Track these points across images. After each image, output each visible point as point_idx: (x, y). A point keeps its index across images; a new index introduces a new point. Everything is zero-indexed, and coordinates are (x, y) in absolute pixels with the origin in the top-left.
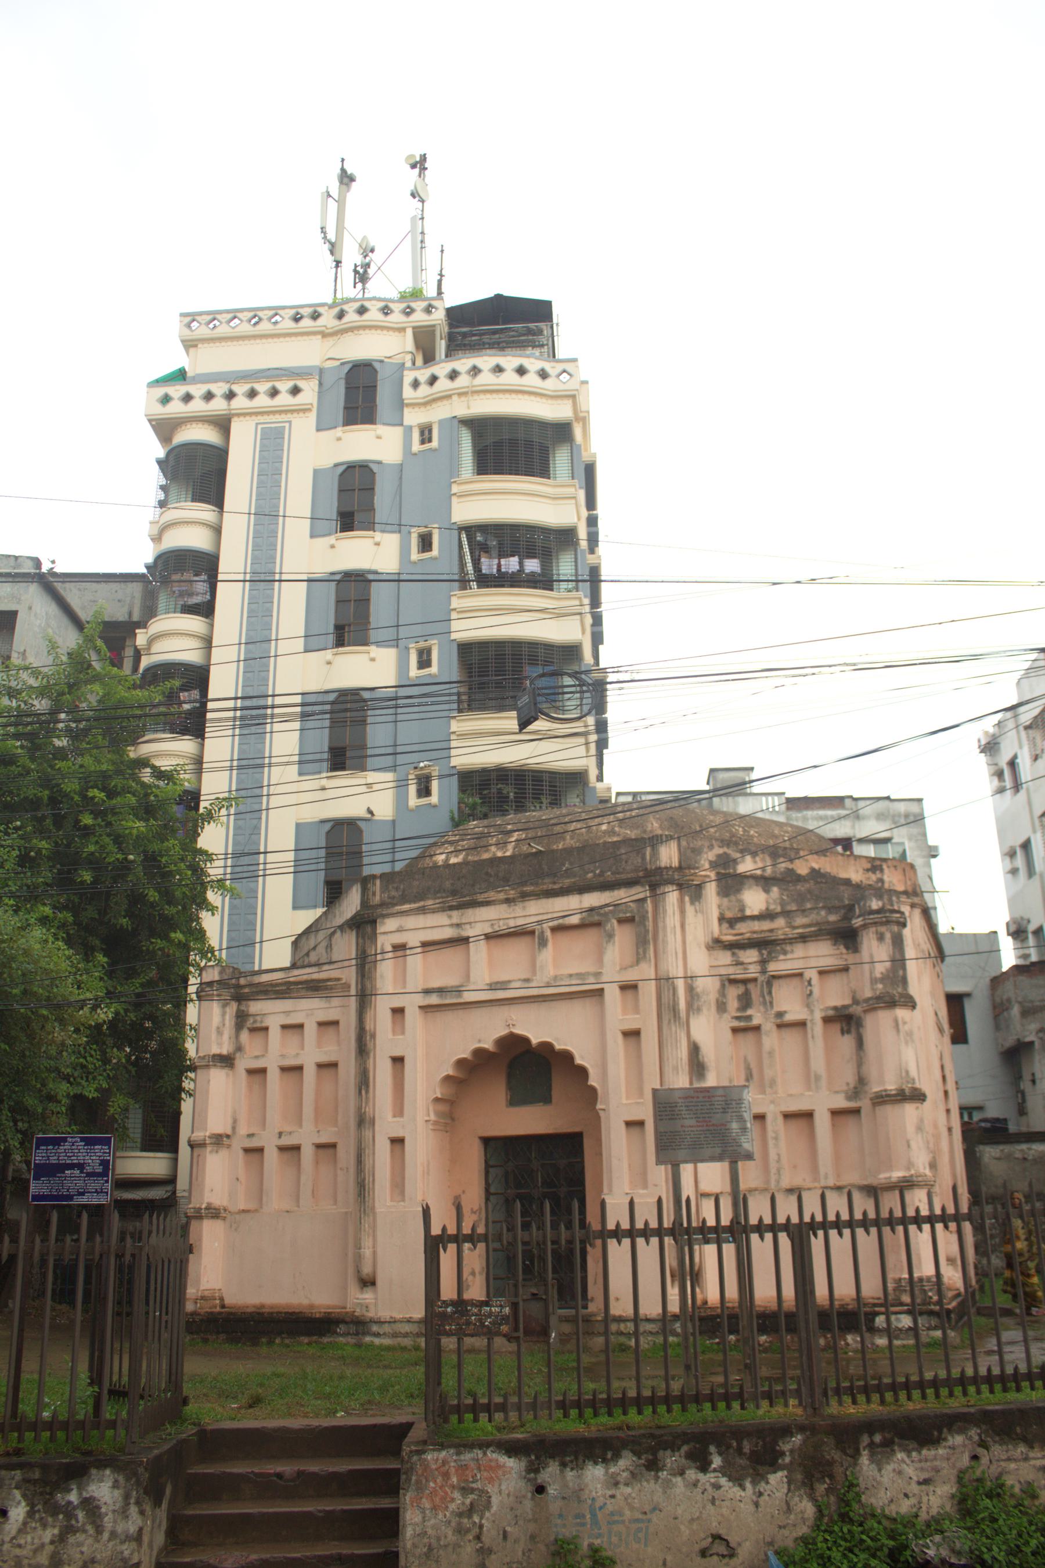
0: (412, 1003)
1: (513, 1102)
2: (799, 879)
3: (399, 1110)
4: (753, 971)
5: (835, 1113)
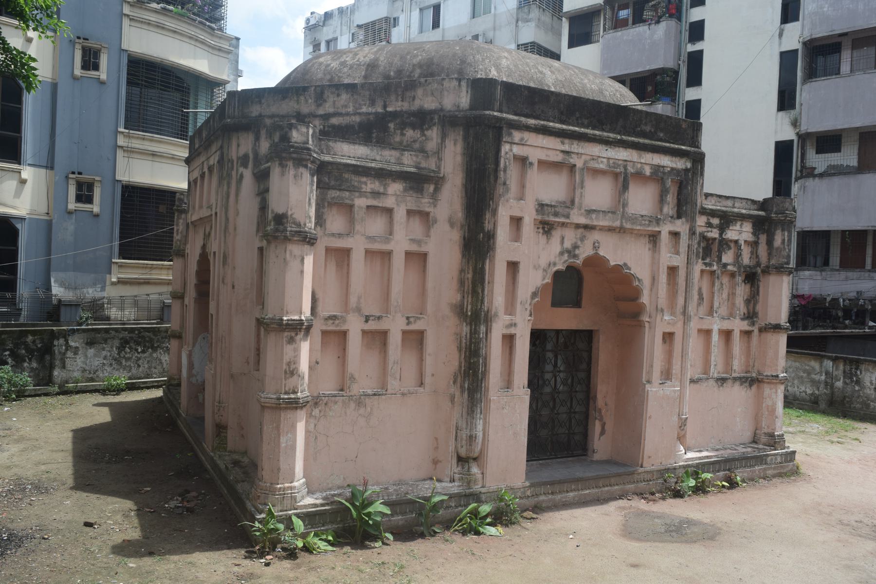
0: (529, 217)
3: (510, 309)
4: (714, 234)
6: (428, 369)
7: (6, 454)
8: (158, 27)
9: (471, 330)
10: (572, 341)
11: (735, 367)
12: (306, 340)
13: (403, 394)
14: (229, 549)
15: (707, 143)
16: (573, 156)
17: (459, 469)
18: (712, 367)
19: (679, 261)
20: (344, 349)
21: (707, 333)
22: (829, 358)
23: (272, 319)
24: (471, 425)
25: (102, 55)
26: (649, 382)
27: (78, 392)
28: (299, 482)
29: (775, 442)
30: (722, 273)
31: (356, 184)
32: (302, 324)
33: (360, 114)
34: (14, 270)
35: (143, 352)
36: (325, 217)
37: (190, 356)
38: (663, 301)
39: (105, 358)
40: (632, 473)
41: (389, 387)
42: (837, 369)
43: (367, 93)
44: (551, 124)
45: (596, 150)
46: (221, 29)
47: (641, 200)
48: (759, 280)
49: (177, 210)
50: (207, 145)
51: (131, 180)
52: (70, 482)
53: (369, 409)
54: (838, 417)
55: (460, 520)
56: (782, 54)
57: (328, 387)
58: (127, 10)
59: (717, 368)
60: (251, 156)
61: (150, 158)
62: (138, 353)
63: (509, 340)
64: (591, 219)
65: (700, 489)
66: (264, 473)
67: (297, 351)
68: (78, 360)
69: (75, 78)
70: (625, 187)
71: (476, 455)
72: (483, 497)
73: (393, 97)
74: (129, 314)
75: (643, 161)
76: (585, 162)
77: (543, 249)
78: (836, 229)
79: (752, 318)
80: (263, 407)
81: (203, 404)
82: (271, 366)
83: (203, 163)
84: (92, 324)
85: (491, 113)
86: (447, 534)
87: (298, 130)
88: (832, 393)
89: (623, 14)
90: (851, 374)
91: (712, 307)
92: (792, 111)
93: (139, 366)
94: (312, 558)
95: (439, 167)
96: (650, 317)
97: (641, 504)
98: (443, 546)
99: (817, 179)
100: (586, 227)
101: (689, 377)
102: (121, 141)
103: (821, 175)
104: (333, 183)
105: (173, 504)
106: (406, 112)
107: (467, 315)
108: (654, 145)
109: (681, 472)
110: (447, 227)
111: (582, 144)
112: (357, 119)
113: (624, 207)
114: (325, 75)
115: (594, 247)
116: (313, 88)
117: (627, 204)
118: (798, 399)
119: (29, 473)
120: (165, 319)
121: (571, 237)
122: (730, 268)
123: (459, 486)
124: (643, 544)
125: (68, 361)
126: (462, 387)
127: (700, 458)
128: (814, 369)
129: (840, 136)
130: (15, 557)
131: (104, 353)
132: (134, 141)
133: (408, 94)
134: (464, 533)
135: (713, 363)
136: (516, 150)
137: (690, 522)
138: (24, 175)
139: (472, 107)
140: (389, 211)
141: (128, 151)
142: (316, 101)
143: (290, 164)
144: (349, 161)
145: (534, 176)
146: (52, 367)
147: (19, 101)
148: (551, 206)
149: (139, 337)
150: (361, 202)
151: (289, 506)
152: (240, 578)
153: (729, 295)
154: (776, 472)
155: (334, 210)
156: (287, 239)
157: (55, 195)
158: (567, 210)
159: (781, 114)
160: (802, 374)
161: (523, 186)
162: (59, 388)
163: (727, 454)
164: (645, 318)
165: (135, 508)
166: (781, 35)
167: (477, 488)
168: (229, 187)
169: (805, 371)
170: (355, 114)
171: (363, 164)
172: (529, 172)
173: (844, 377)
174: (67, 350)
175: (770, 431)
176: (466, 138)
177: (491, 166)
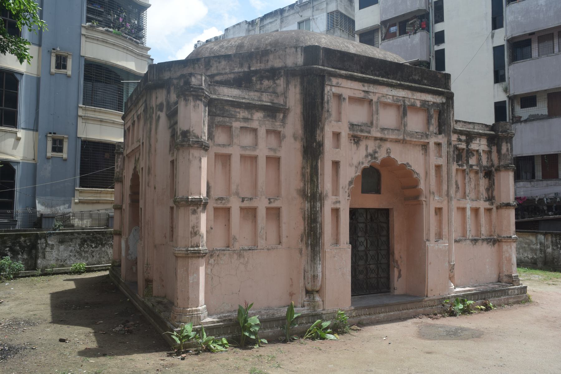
0: (345, 133)
1: (363, 192)
3: (336, 192)
4: (463, 146)
6: (284, 233)
7: (7, 307)
8: (103, 42)
9: (311, 206)
10: (376, 216)
11: (482, 232)
12: (204, 212)
13: (268, 249)
14: (156, 352)
15: (455, 87)
16: (370, 94)
17: (307, 298)
18: (468, 232)
19: (442, 161)
20: (229, 220)
21: (463, 210)
22: (541, 233)
23: (182, 198)
24: (314, 268)
25: (68, 59)
26: (428, 240)
27: (53, 274)
28: (202, 307)
29: (513, 281)
30: (470, 171)
31: (233, 113)
32: (201, 201)
33: (233, 73)
34: (11, 195)
35: (96, 247)
36: (214, 134)
37: (127, 242)
38: (433, 187)
39: (71, 251)
40: (421, 301)
41: (259, 245)
42: (547, 240)
43: (238, 60)
44: (356, 74)
45: (385, 90)
46: (142, 43)
47: (415, 122)
48: (493, 176)
49: (117, 153)
50: (136, 104)
51: (87, 137)
52: (50, 319)
53: (246, 259)
54: (551, 271)
55: (310, 331)
56: (495, 48)
57: (219, 244)
58: (84, 31)
59: (471, 234)
60: (165, 103)
61: (99, 123)
62: (93, 248)
63: (336, 212)
64: (384, 134)
65: (466, 311)
66: (179, 301)
67: (198, 219)
68: (54, 253)
69: (51, 74)
70: (405, 114)
71: (318, 289)
72: (324, 317)
73: (254, 61)
74: (86, 223)
75: (415, 98)
76: (378, 98)
77: (355, 153)
78: (538, 154)
79: (491, 200)
80: (177, 257)
81: (136, 273)
82: (181, 231)
83: (134, 115)
84: (62, 230)
85: (317, 66)
86: (302, 340)
87: (195, 77)
88: (546, 256)
89: (393, 29)
90: (557, 243)
91: (465, 193)
92: (504, 83)
93: (93, 256)
94: (213, 355)
95: (286, 103)
96: (426, 198)
97: (429, 321)
98: (299, 346)
99: (523, 123)
100: (381, 139)
101: (454, 239)
102: (81, 113)
103: (526, 121)
104: (218, 112)
105: (118, 329)
106: (263, 70)
107: (308, 196)
108: (422, 88)
109: (453, 300)
110: (292, 140)
111: (376, 86)
112: (232, 76)
113: (404, 127)
114: (210, 54)
115: (387, 152)
116: (203, 59)
117: (407, 125)
118: (523, 262)
119: (22, 316)
120: (110, 225)
121: (372, 146)
122: (474, 167)
123: (308, 310)
124: (433, 341)
125: (47, 253)
126: (307, 243)
127: (465, 291)
128: (532, 241)
129: (535, 96)
130: (13, 360)
131: (70, 248)
132: (89, 112)
133: (264, 59)
134: (313, 339)
135: (468, 230)
136: (334, 90)
137: (463, 329)
138: (19, 135)
139: (305, 63)
140: (255, 131)
141: (85, 119)
142: (205, 67)
143: (191, 98)
144: (228, 98)
145: (346, 105)
146: (36, 258)
147: (16, 88)
148: (358, 125)
149: (93, 237)
150: (236, 125)
151: (196, 323)
152: (165, 366)
153: (475, 185)
154: (515, 300)
155: (220, 130)
156: (190, 146)
157: (39, 148)
158: (369, 128)
159: (496, 85)
160: (524, 245)
161: (339, 113)
162: (42, 271)
163: (482, 288)
164: (423, 199)
165: (93, 331)
166: (493, 37)
167: (319, 310)
168: (151, 124)
169: (526, 243)
170: (230, 73)
171: (237, 100)
172: (343, 104)
173: (552, 246)
174: (46, 246)
175: (509, 273)
176: (302, 83)
177: (319, 101)
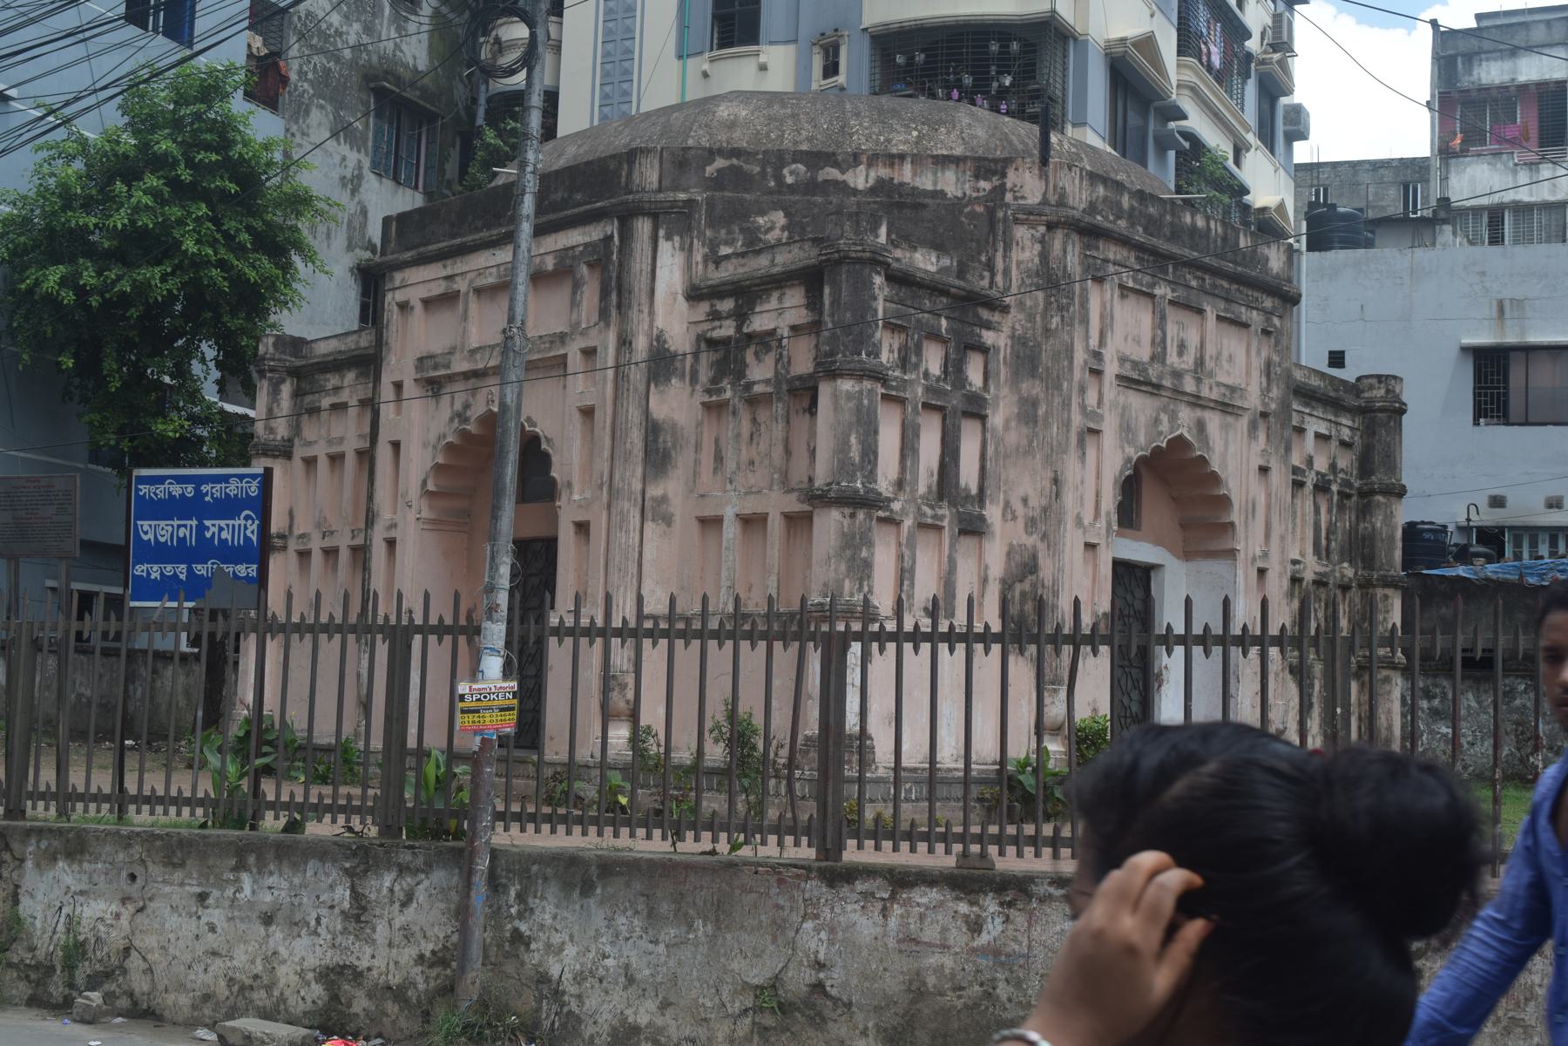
0: (408, 376)
2: (855, 192)
4: (727, 329)
5: (790, 518)
18: (723, 590)
